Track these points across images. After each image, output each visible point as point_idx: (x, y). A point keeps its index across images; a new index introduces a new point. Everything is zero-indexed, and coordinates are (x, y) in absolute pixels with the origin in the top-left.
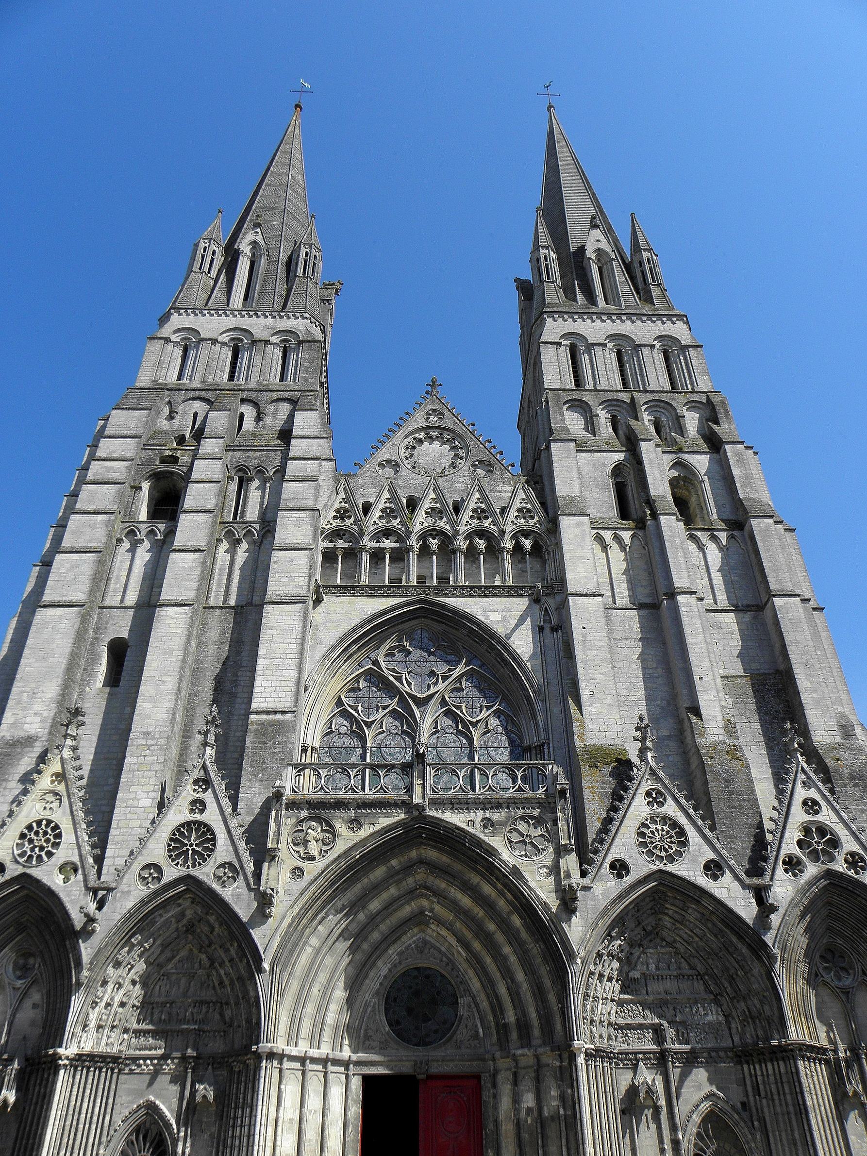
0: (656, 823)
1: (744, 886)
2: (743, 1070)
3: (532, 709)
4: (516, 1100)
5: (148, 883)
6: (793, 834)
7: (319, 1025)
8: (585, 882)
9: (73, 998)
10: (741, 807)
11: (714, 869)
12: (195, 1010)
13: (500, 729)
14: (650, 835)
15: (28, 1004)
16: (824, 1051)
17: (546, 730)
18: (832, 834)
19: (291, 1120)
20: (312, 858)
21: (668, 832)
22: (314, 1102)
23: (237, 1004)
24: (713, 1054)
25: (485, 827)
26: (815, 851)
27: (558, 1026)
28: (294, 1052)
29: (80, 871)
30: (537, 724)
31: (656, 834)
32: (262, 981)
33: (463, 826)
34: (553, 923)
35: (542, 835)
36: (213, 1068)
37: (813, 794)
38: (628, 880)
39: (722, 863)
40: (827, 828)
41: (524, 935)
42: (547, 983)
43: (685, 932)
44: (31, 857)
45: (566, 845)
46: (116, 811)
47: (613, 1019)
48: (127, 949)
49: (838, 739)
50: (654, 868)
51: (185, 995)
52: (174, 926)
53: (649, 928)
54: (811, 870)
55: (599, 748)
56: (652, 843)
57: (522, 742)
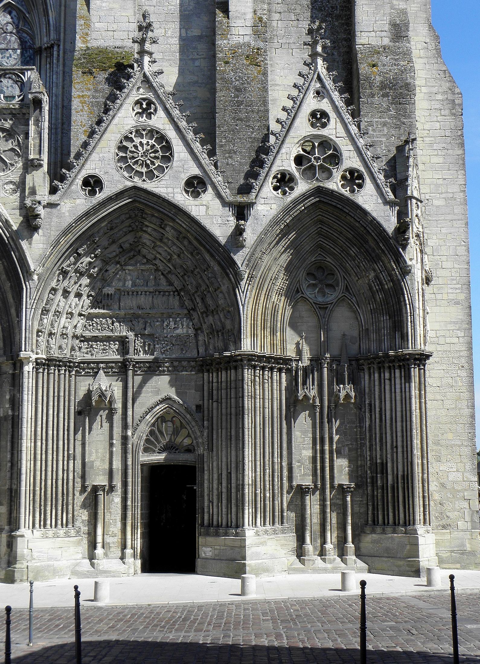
0: (142, 136)
1: (225, 203)
2: (203, 377)
10: (248, 119)
11: (195, 186)
13: (10, 28)
14: (133, 149)
16: (287, 361)
17: (57, 30)
18: (335, 149)
21: (153, 146)
24: (176, 364)
26: (312, 167)
31: (140, 148)
34: (13, 240)
35: (12, 150)
37: (325, 105)
38: (100, 196)
39: (206, 180)
40: (331, 143)
43: (162, 250)
45: (33, 160)
47: (79, 332)
49: (386, 41)
50: (129, 184)
53: (126, 246)
55: (102, 51)
56: (133, 158)
57: (34, 43)
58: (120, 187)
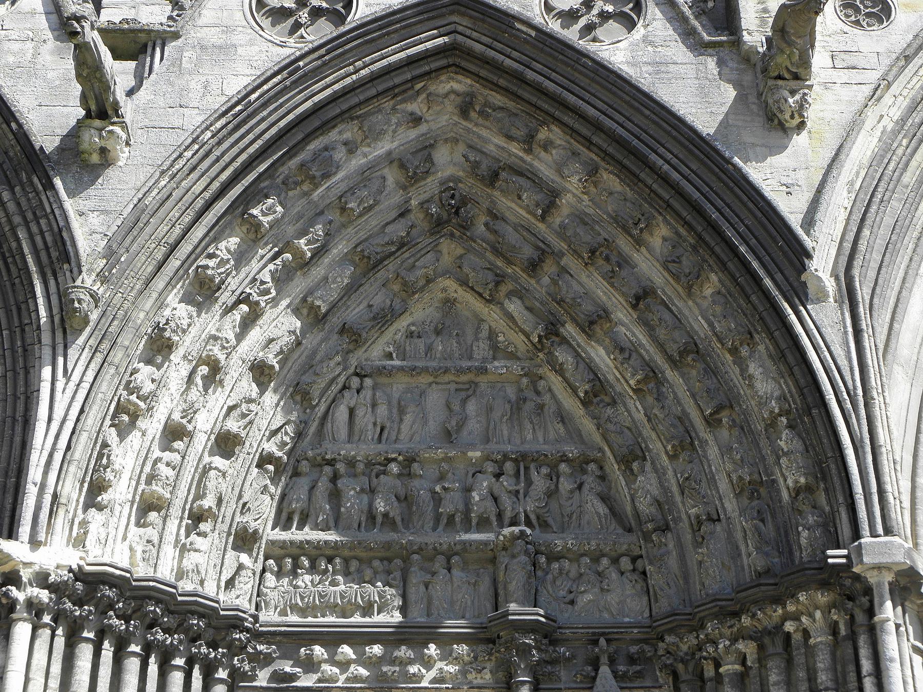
5: (297, 26)
9: (46, 372)
12: (506, 482)
23: (686, 444)
32: (822, 325)
36: (615, 673)
48: (233, 242)
51: (448, 436)
52: (392, 199)
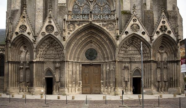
3: (113, 3)
4: (106, 68)
6: (159, 27)
7: (75, 57)
8: (121, 35)
11: (143, 33)
15: (27, 54)
19: (71, 70)
20: (71, 31)
22: (74, 68)
25: (103, 25)
27: (114, 58)
28: (71, 61)
29: (31, 33)
30: (114, 7)
32: (65, 51)
33: (99, 25)
38: (128, 35)
41: (109, 44)
42: (112, 51)
44: (22, 31)
46: (36, 23)
50: (133, 33)
54: (161, 34)
58: (131, 33)
